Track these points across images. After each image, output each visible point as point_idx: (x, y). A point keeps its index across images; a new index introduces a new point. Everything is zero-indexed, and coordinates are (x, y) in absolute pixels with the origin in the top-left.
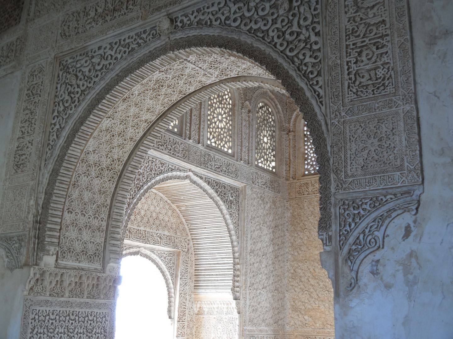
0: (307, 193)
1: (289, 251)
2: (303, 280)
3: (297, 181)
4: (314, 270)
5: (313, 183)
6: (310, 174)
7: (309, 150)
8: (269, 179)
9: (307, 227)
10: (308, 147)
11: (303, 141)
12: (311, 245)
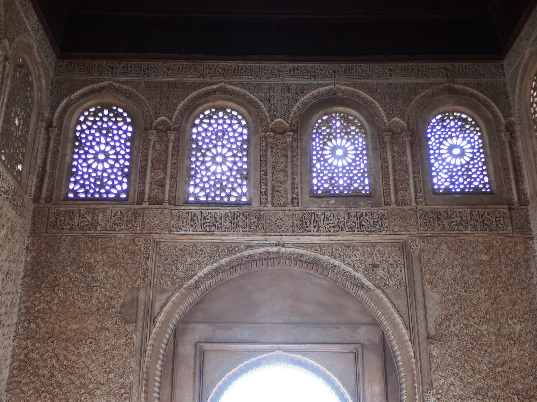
0: (69, 227)
1: (21, 320)
2: (41, 372)
3: (53, 206)
4: (65, 356)
5: (82, 212)
6: (77, 198)
7: (80, 161)
8: (13, 187)
9: (61, 282)
10: (80, 157)
11: (69, 146)
12: (65, 313)
